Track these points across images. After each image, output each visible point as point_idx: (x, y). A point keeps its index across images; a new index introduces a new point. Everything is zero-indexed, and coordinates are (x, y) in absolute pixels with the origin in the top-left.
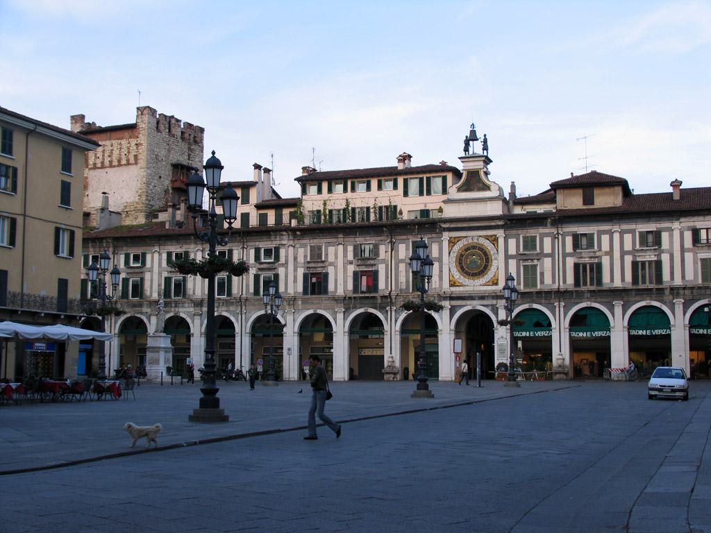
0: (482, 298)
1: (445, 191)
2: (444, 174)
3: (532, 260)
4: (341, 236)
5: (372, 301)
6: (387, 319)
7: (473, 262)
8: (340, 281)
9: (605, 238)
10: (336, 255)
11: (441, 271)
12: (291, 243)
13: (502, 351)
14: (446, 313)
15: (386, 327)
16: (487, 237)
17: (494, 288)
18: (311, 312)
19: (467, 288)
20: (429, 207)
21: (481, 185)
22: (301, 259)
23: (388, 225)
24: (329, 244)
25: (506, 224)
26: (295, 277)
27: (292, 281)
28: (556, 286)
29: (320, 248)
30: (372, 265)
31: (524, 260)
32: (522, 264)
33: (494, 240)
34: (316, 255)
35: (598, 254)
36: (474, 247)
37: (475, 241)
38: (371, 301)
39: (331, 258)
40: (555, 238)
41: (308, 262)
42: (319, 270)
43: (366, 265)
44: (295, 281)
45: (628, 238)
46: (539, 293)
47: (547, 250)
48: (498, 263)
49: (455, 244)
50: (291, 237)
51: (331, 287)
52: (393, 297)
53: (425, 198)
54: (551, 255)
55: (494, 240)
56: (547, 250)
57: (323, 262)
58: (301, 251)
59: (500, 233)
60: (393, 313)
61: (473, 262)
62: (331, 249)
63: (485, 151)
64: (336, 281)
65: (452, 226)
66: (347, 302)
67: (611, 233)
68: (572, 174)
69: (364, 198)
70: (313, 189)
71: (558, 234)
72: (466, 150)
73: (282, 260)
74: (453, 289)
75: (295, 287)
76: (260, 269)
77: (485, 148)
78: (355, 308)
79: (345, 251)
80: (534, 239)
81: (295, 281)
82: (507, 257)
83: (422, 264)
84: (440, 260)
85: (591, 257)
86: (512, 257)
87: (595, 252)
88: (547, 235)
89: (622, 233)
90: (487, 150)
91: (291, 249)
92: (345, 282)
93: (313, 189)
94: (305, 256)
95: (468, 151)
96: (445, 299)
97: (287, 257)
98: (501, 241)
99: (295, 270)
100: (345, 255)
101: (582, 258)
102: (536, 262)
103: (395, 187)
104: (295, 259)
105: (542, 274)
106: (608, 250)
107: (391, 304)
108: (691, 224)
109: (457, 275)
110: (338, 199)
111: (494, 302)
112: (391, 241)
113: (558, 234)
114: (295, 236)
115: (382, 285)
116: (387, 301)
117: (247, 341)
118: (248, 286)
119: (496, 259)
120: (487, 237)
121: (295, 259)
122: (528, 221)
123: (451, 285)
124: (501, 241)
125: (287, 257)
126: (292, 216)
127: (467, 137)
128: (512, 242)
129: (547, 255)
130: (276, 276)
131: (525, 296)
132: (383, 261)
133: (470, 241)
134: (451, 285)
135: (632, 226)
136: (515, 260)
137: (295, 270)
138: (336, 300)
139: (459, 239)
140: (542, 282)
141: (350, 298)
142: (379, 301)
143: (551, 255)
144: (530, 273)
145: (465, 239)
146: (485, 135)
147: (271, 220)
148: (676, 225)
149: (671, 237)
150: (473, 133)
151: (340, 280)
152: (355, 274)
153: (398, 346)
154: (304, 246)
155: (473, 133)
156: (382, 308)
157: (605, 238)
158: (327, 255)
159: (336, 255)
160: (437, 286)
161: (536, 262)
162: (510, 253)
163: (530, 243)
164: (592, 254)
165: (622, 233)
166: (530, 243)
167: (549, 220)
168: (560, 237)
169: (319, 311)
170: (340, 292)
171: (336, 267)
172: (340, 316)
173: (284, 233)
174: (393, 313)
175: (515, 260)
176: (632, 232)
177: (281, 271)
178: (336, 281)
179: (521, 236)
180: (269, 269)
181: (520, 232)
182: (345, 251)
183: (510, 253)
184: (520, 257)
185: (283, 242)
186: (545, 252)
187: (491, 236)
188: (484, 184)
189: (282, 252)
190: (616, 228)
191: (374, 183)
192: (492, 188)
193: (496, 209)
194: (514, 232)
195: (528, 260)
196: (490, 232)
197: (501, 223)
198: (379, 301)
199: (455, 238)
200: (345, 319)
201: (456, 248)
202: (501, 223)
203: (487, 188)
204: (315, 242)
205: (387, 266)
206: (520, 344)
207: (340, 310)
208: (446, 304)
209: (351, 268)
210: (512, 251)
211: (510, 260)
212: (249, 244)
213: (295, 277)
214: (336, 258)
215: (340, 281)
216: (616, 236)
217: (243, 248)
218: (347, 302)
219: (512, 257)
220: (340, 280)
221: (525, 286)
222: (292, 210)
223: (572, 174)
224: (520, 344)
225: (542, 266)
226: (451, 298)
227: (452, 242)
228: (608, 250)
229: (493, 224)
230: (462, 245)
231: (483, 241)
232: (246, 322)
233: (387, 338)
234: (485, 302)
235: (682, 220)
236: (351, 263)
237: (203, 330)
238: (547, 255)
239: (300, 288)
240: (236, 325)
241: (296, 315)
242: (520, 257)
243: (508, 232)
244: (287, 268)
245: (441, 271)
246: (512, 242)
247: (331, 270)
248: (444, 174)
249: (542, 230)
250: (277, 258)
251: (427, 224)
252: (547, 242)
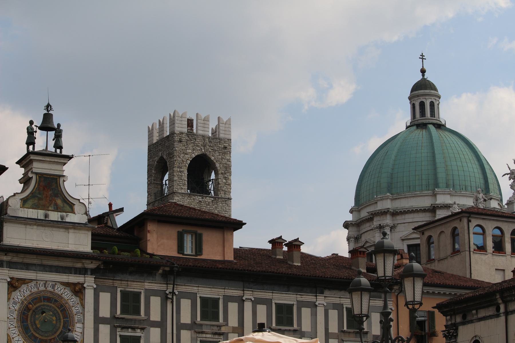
3: (134, 329)
9: (233, 307)
16: (67, 285)
21: (59, 202)
31: (123, 328)
32: (119, 332)
33: (78, 290)
35: (223, 329)
36: (48, 299)
37: (50, 289)
40: (165, 298)
45: (262, 309)
47: (155, 316)
55: (78, 290)
56: (155, 316)
59: (89, 281)
63: (58, 151)
65: (15, 259)
67: (241, 301)
68: (110, 205)
71: (173, 293)
72: (31, 141)
77: (58, 146)
82: (98, 320)
85: (215, 334)
86: (104, 321)
87: (220, 326)
88: (155, 293)
89: (256, 302)
90: (61, 148)
95: (33, 144)
101: (203, 333)
102: (138, 333)
106: (236, 325)
108: (337, 301)
119: (79, 321)
124: (89, 295)
127: (31, 123)
128: (105, 298)
129: (155, 324)
133: (42, 288)
135: (266, 295)
136: (109, 326)
139: (24, 281)
143: (161, 324)
145: (33, 284)
146: (59, 125)
148: (321, 300)
149: (314, 315)
150: (47, 117)
155: (47, 117)
157: (233, 307)
161: (138, 333)
162: (101, 315)
163: (131, 302)
164: (216, 330)
165: (256, 302)
166: (131, 302)
167: (161, 271)
168: (175, 297)
175: (109, 326)
176: (268, 302)
179: (119, 290)
181: (117, 283)
183: (101, 315)
184: (114, 321)
186: (152, 318)
187: (75, 285)
188: (65, 200)
190: (248, 295)
192: (76, 208)
193: (81, 243)
194: (109, 282)
195: (127, 328)
196: (74, 279)
197: (92, 265)
199: (18, 280)
201: (19, 296)
202: (92, 265)
210: (105, 312)
211: (102, 327)
216: (248, 306)
219: (104, 321)
223: (110, 205)
228: (236, 325)
229: (79, 265)
230: (29, 293)
231: (60, 290)
235: (327, 293)
249: (148, 285)
252: (156, 302)
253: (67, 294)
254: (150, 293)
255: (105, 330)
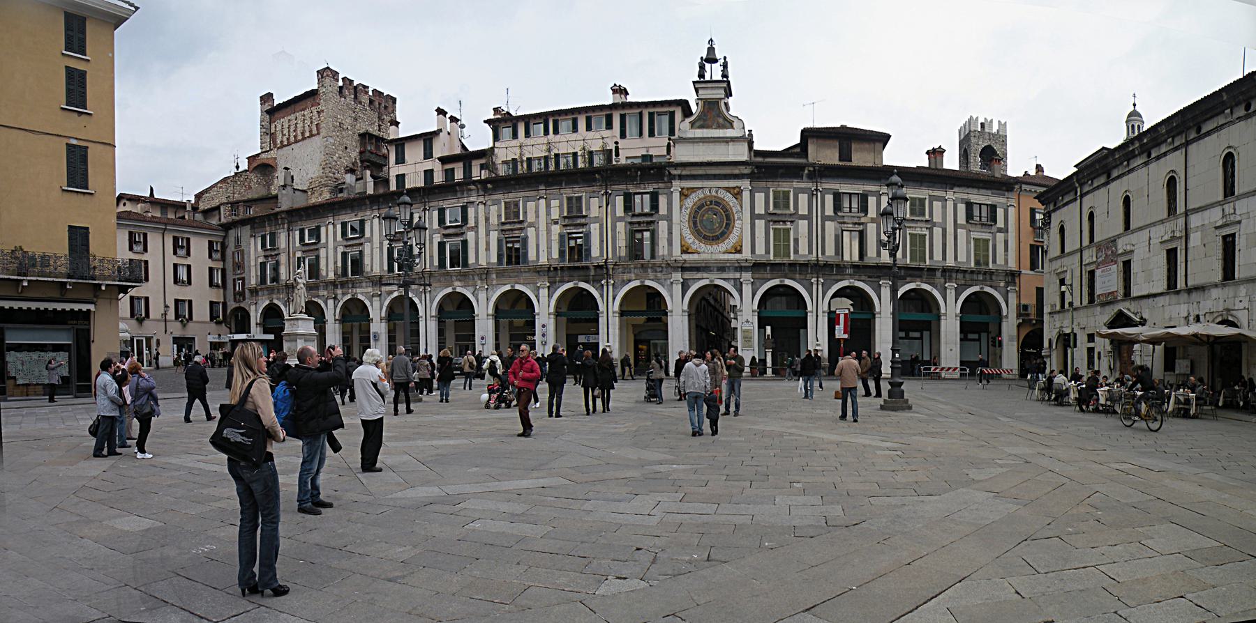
0: (722, 269)
1: (672, 132)
2: (671, 109)
3: (784, 222)
4: (542, 187)
5: (581, 272)
6: (602, 296)
7: (712, 222)
8: (543, 247)
10: (537, 212)
11: (670, 233)
12: (481, 199)
13: (748, 339)
14: (677, 289)
15: (602, 307)
16: (727, 189)
17: (738, 256)
18: (508, 288)
19: (703, 256)
20: (652, 152)
22: (494, 220)
23: (604, 174)
24: (527, 199)
25: (753, 173)
26: (488, 244)
27: (484, 249)
28: (813, 257)
29: (517, 205)
30: (583, 225)
31: (775, 222)
33: (737, 193)
34: (513, 215)
38: (582, 273)
39: (531, 218)
40: (812, 194)
41: (503, 224)
42: (516, 233)
43: (576, 226)
44: (488, 249)
46: (792, 265)
48: (742, 225)
49: (687, 196)
50: (481, 193)
51: (532, 255)
52: (610, 267)
53: (647, 141)
54: (808, 217)
55: (737, 193)
57: (521, 222)
58: (494, 209)
59: (745, 184)
60: (611, 288)
61: (712, 222)
62: (531, 205)
64: (538, 246)
66: (553, 274)
69: (568, 143)
70: (506, 132)
71: (817, 190)
73: (471, 223)
74: (685, 257)
75: (488, 256)
76: (445, 236)
78: (563, 282)
79: (548, 206)
80: (786, 195)
81: (488, 249)
82: (754, 217)
83: (642, 225)
84: (669, 218)
86: (760, 217)
88: (803, 191)
91: (481, 207)
92: (549, 248)
93: (506, 132)
94: (499, 216)
96: (675, 269)
97: (476, 218)
98: (746, 195)
99: (487, 235)
100: (548, 213)
102: (789, 225)
103: (609, 126)
104: (487, 219)
105: (796, 241)
107: (608, 276)
109: (690, 239)
110: (535, 146)
111: (737, 275)
112: (606, 193)
113: (817, 190)
114: (486, 190)
115: (595, 252)
116: (601, 272)
117: (433, 326)
118: (431, 257)
120: (727, 189)
121: (487, 219)
122: (781, 171)
123: (684, 252)
124: (746, 195)
125: (476, 218)
126: (482, 167)
128: (760, 197)
129: (803, 217)
130: (465, 243)
131: (775, 268)
132: (596, 220)
134: (684, 252)
137: (487, 235)
138: (538, 270)
140: (796, 251)
141: (555, 269)
142: (592, 273)
143: (808, 217)
144: (782, 238)
147: (459, 176)
151: (543, 245)
152: (561, 236)
153: (617, 331)
154: (497, 203)
156: (595, 281)
158: (525, 213)
159: (537, 212)
160: (666, 253)
163: (782, 200)
166: (782, 200)
169: (518, 287)
170: (543, 260)
171: (537, 230)
172: (544, 293)
173: (473, 187)
174: (611, 288)
177: (470, 236)
178: (538, 246)
180: (456, 235)
181: (769, 184)
182: (548, 206)
185: (472, 199)
189: (471, 211)
191: (582, 124)
193: (739, 153)
197: (747, 171)
198: (592, 273)
200: (550, 296)
201: (689, 202)
202: (747, 171)
203: (730, 124)
204: (511, 197)
205: (601, 226)
206: (769, 329)
207: (544, 282)
208: (677, 276)
209: (556, 229)
210: (760, 209)
212: (432, 204)
213: (488, 244)
214: (537, 216)
215: (543, 247)
217: (425, 210)
218: (553, 274)
219: (760, 217)
220: (543, 245)
221: (775, 256)
222: (483, 161)
224: (769, 329)
225: (796, 232)
226: (684, 269)
227: (684, 195)
229: (737, 172)
231: (722, 194)
232: (432, 302)
233: (602, 321)
234: (725, 275)
236: (556, 223)
237: (383, 315)
238: (803, 217)
239: (494, 259)
240: (419, 306)
241: (490, 293)
242: (770, 218)
243: (755, 184)
244: (477, 232)
245: (670, 233)
246: (760, 197)
247: (531, 232)
248: (671, 109)
249: (796, 184)
250: (465, 219)
251: (654, 172)
253: (728, 197)
254: (798, 191)
255: (760, 224)
